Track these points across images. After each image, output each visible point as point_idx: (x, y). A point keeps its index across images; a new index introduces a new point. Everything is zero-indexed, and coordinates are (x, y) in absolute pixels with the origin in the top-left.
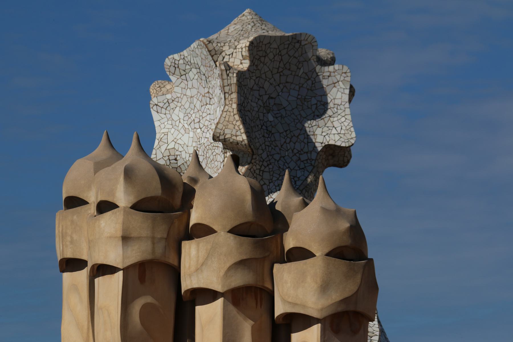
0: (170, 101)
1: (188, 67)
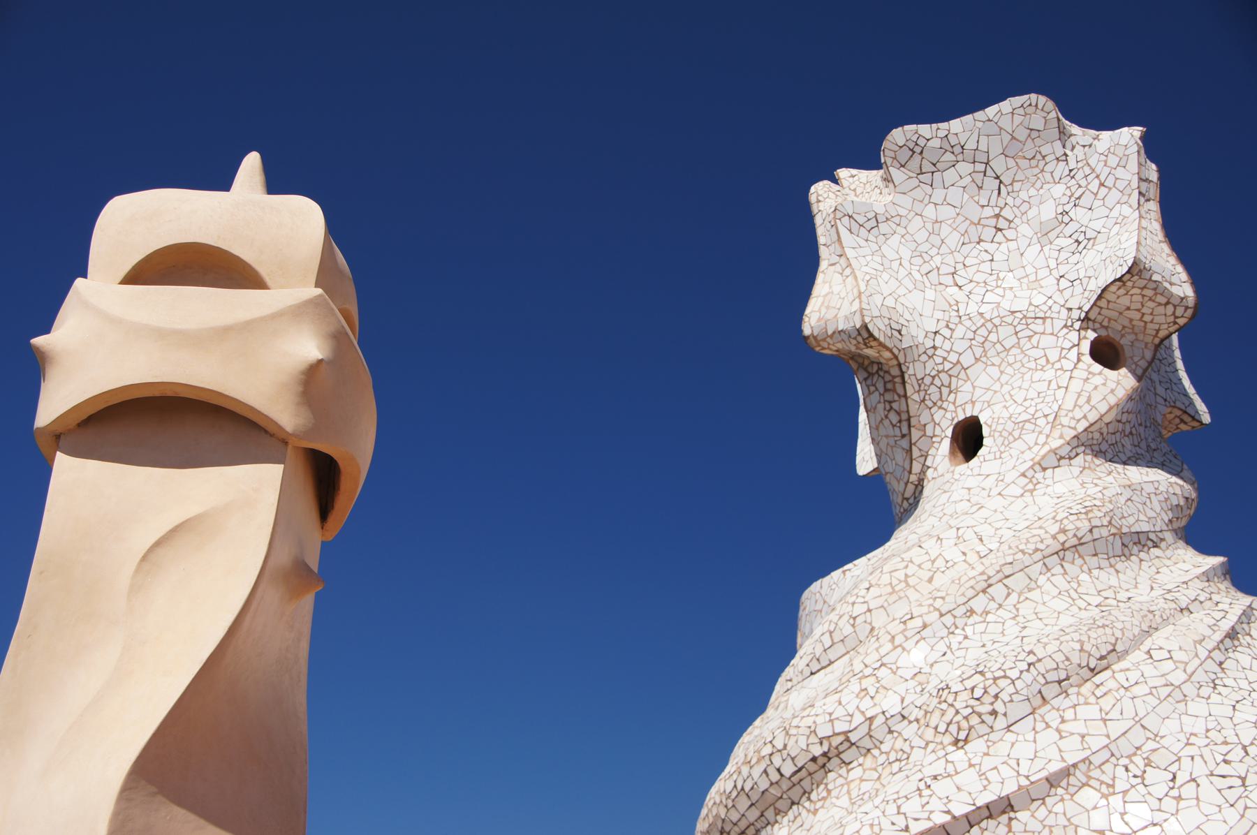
1: (949, 157)
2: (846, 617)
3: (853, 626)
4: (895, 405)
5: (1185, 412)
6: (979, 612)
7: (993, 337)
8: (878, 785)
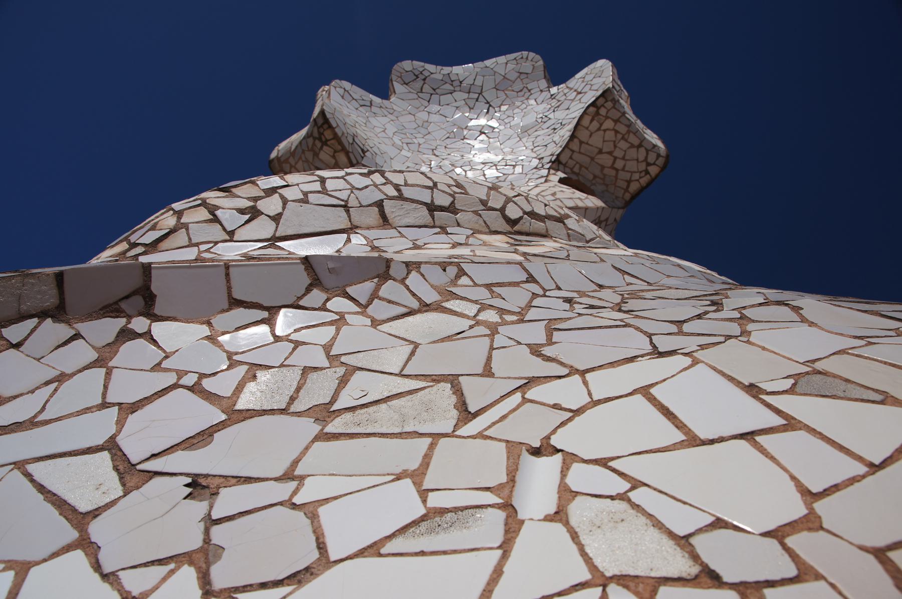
1: (448, 87)
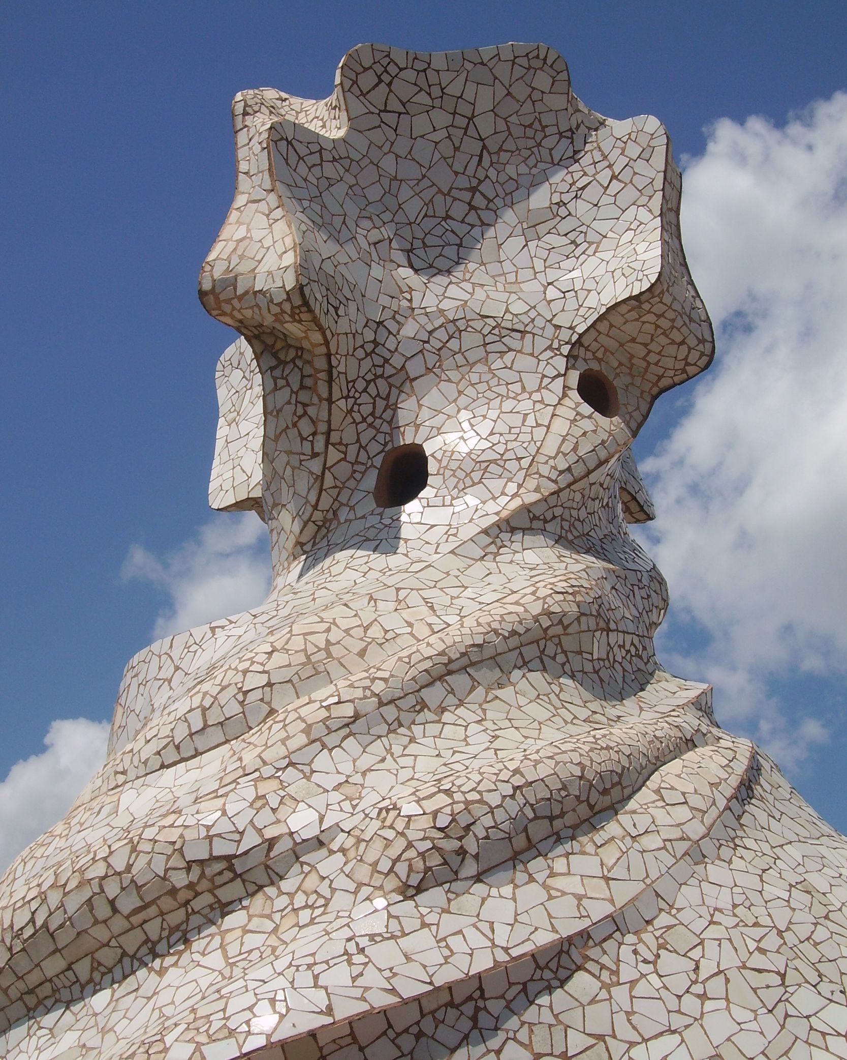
0: (327, 156)
1: (423, 98)
2: (232, 690)
3: (242, 703)
4: (311, 411)
5: (634, 499)
6: (432, 707)
7: (453, 344)
8: (273, 941)
